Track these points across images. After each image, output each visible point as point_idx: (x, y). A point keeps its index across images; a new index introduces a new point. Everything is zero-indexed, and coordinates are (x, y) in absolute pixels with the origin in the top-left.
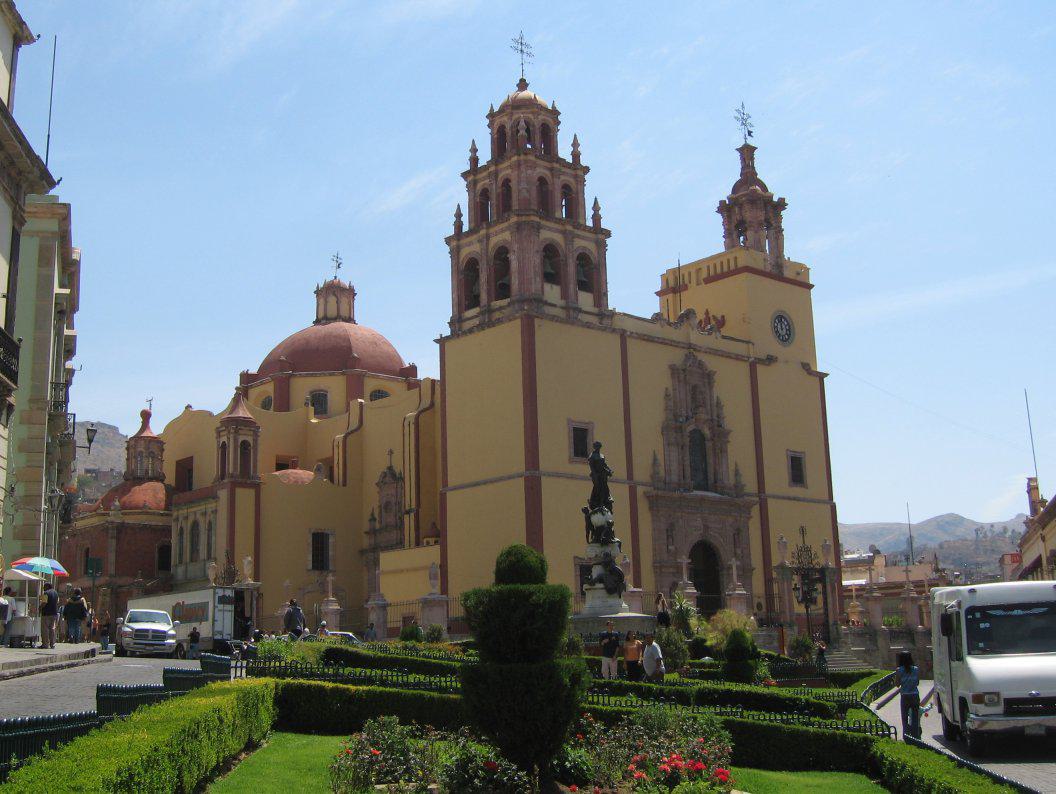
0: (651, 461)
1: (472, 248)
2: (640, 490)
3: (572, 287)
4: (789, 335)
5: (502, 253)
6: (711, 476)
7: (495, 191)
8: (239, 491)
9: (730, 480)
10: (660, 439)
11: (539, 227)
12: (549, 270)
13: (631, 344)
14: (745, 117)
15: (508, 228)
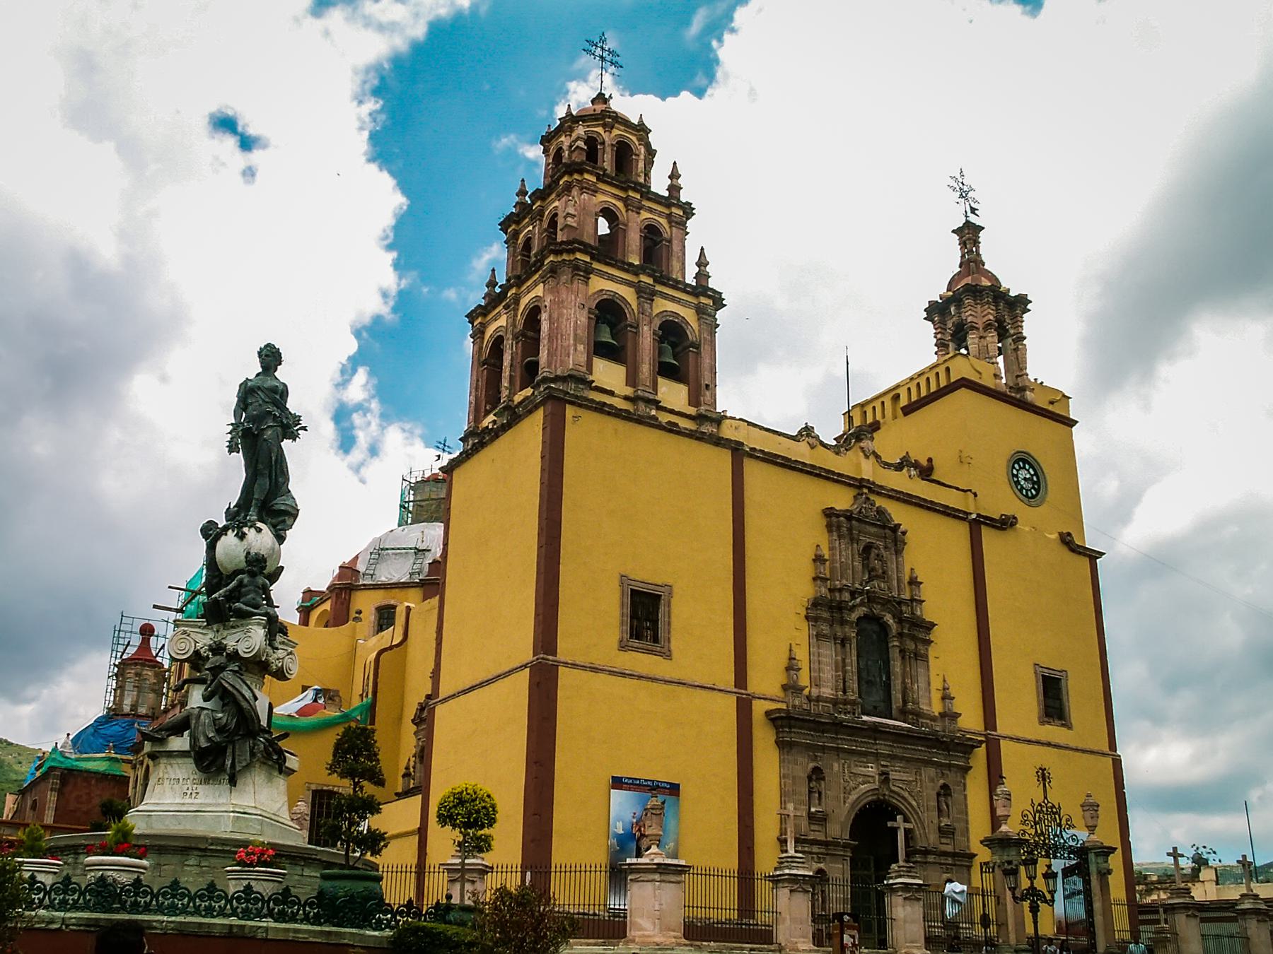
0: (784, 662)
2: (759, 708)
3: (646, 369)
4: (1038, 491)
6: (897, 696)
11: (588, 272)
12: (606, 337)
14: (965, 189)
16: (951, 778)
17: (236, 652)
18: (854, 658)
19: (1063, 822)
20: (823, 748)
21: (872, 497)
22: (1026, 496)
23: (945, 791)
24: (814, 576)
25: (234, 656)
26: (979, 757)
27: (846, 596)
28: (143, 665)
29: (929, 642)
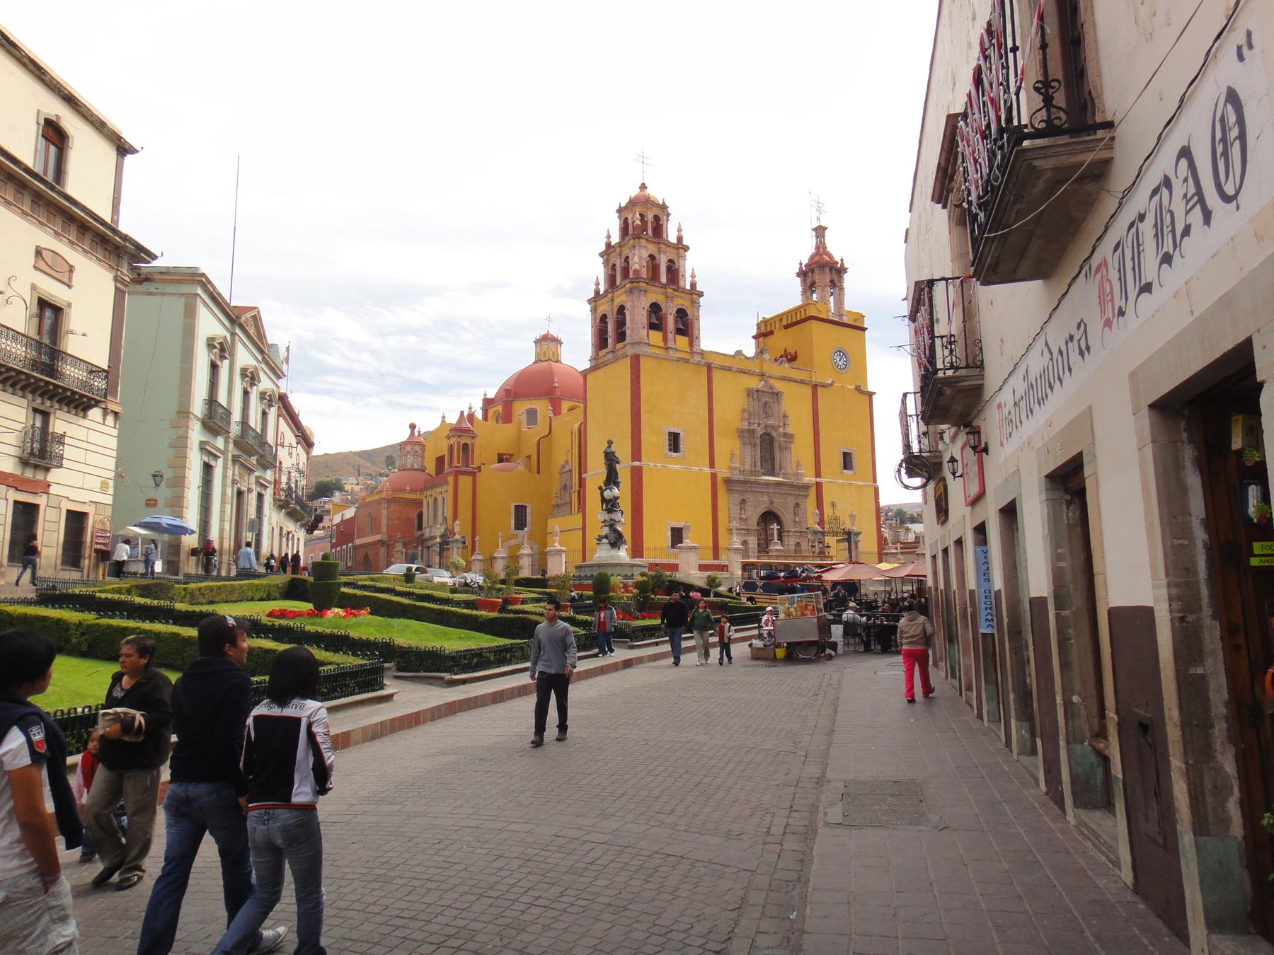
1: (604, 308)
6: (777, 466)
7: (619, 264)
8: (461, 477)
13: (717, 375)
15: (625, 292)
16: (800, 500)
20: (746, 491)
27: (756, 425)
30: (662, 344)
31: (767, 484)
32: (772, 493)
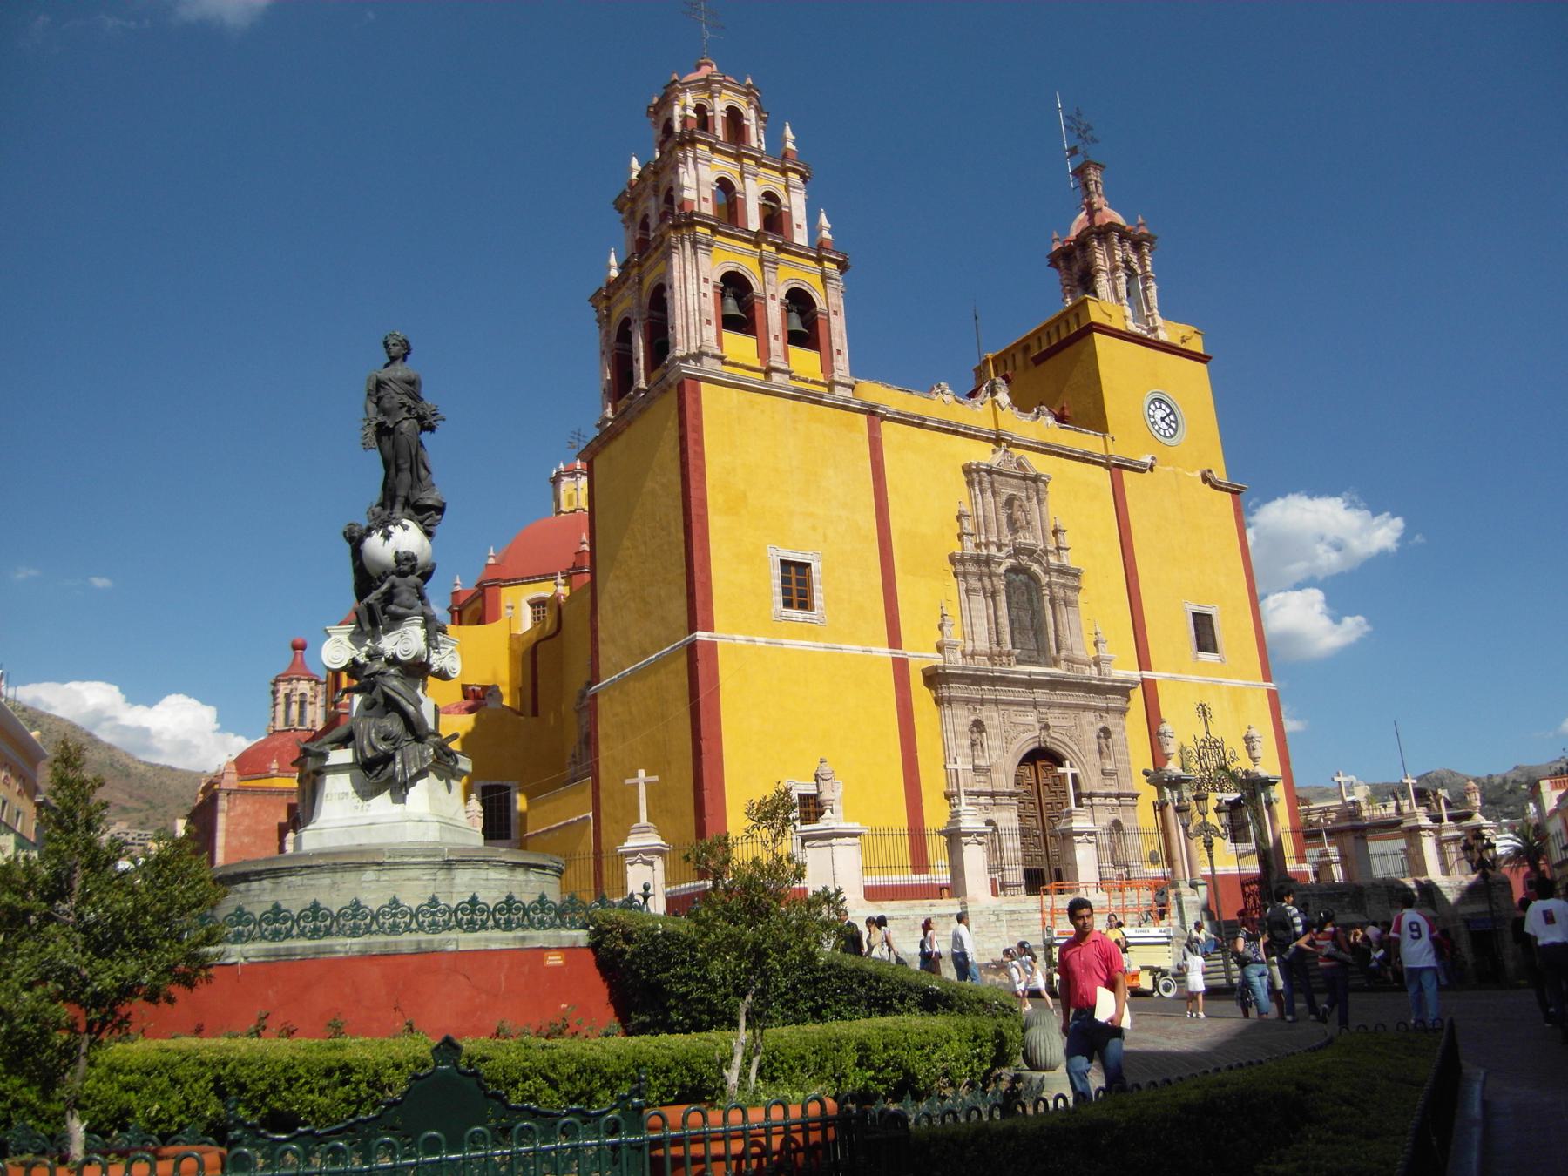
1: (626, 304)
4: (1175, 430)
5: (659, 301)
7: (652, 206)
9: (1086, 652)
10: (953, 587)
13: (888, 430)
16: (1111, 721)
17: (395, 656)
18: (1006, 610)
19: (1227, 756)
20: (982, 702)
21: (1010, 449)
22: (1165, 436)
23: (1106, 732)
24: (959, 531)
25: (393, 661)
26: (1137, 696)
27: (993, 550)
28: (298, 680)
29: (1077, 589)
30: (756, 364)
31: (1031, 684)
32: (1050, 705)
